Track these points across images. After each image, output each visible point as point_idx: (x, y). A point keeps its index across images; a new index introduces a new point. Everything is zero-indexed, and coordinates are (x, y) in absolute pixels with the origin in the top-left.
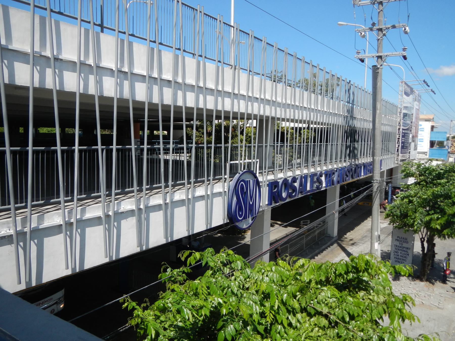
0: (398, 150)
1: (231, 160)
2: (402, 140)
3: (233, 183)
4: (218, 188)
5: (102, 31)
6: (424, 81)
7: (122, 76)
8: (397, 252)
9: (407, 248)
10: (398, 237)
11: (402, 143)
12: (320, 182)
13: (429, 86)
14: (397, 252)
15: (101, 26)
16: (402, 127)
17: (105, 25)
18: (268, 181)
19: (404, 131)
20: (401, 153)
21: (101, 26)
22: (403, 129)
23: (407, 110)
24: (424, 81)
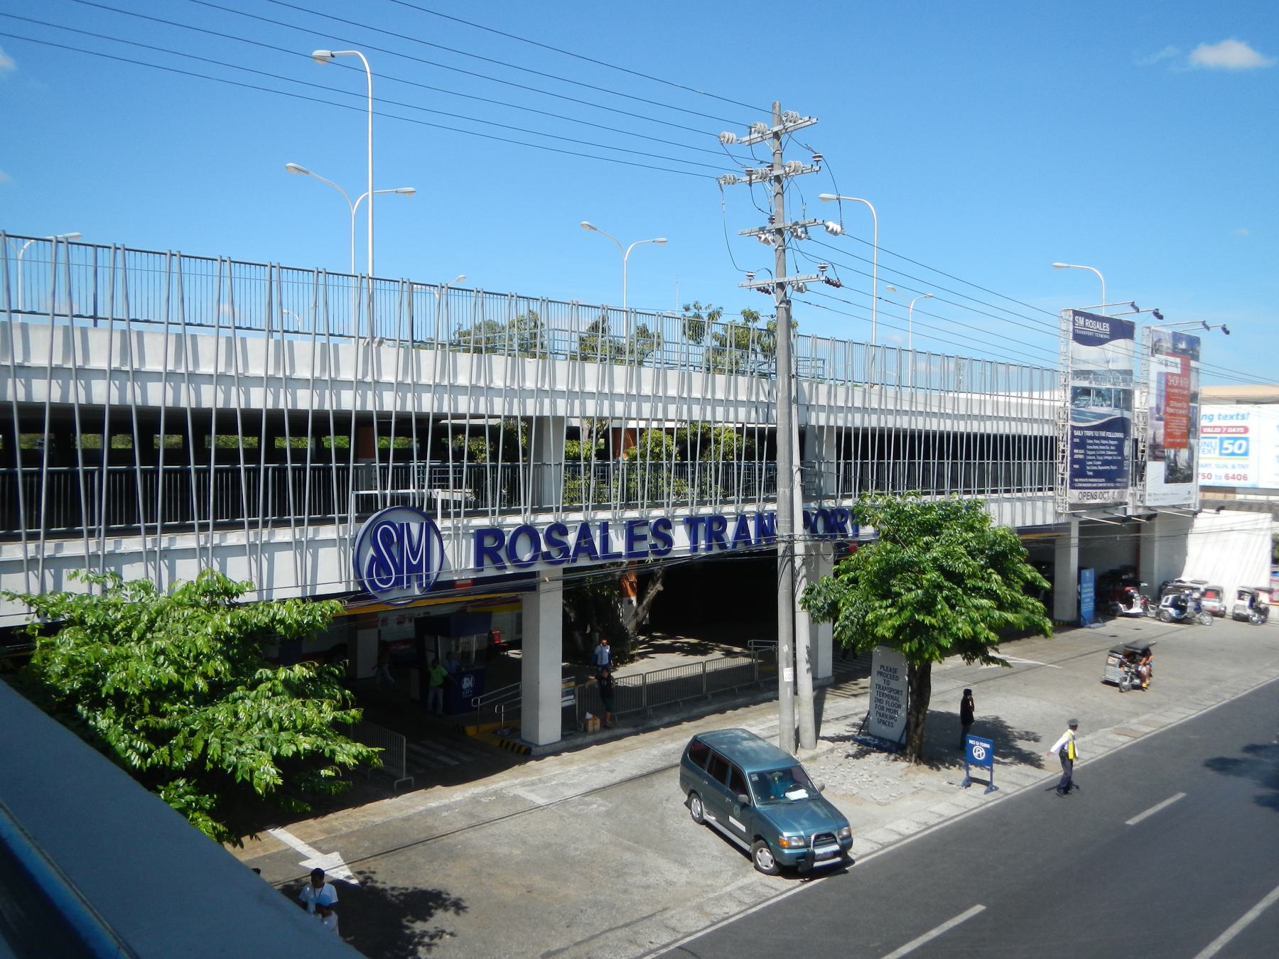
0: (1063, 479)
1: (356, 488)
2: (1072, 454)
3: (364, 525)
4: (328, 532)
5: (95, 325)
6: (1133, 305)
7: (124, 376)
8: (880, 701)
9: (898, 692)
10: (882, 667)
11: (1074, 461)
12: (669, 541)
13: (1161, 317)
14: (880, 701)
15: (95, 318)
16: (1070, 423)
17: (99, 315)
18: (473, 527)
19: (1077, 433)
20: (1072, 487)
21: (95, 318)
22: (1073, 428)
23: (1085, 379)
24: (1133, 305)
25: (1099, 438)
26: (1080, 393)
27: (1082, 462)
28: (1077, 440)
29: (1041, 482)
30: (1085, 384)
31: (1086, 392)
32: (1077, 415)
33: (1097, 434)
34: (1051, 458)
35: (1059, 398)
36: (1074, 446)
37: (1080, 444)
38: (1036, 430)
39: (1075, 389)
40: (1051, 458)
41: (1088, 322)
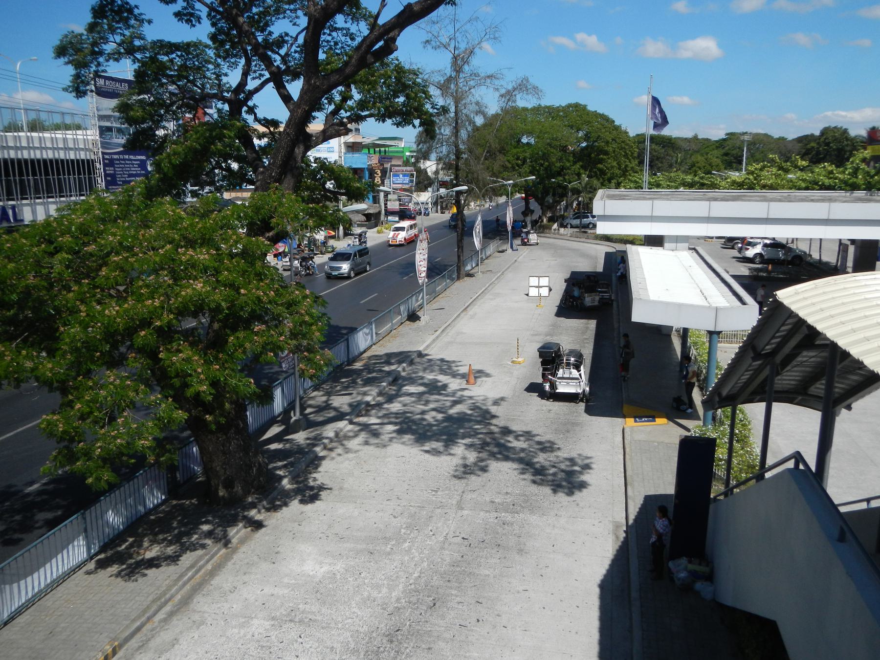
11: (106, 175)
23: (108, 121)
25: (124, 160)
26: (104, 131)
27: (113, 176)
28: (107, 161)
29: (71, 192)
30: (108, 124)
31: (109, 129)
32: (104, 145)
33: (121, 157)
34: (89, 173)
35: (92, 135)
36: (105, 165)
37: (109, 163)
38: (83, 156)
39: (100, 128)
40: (89, 173)
41: (107, 83)
